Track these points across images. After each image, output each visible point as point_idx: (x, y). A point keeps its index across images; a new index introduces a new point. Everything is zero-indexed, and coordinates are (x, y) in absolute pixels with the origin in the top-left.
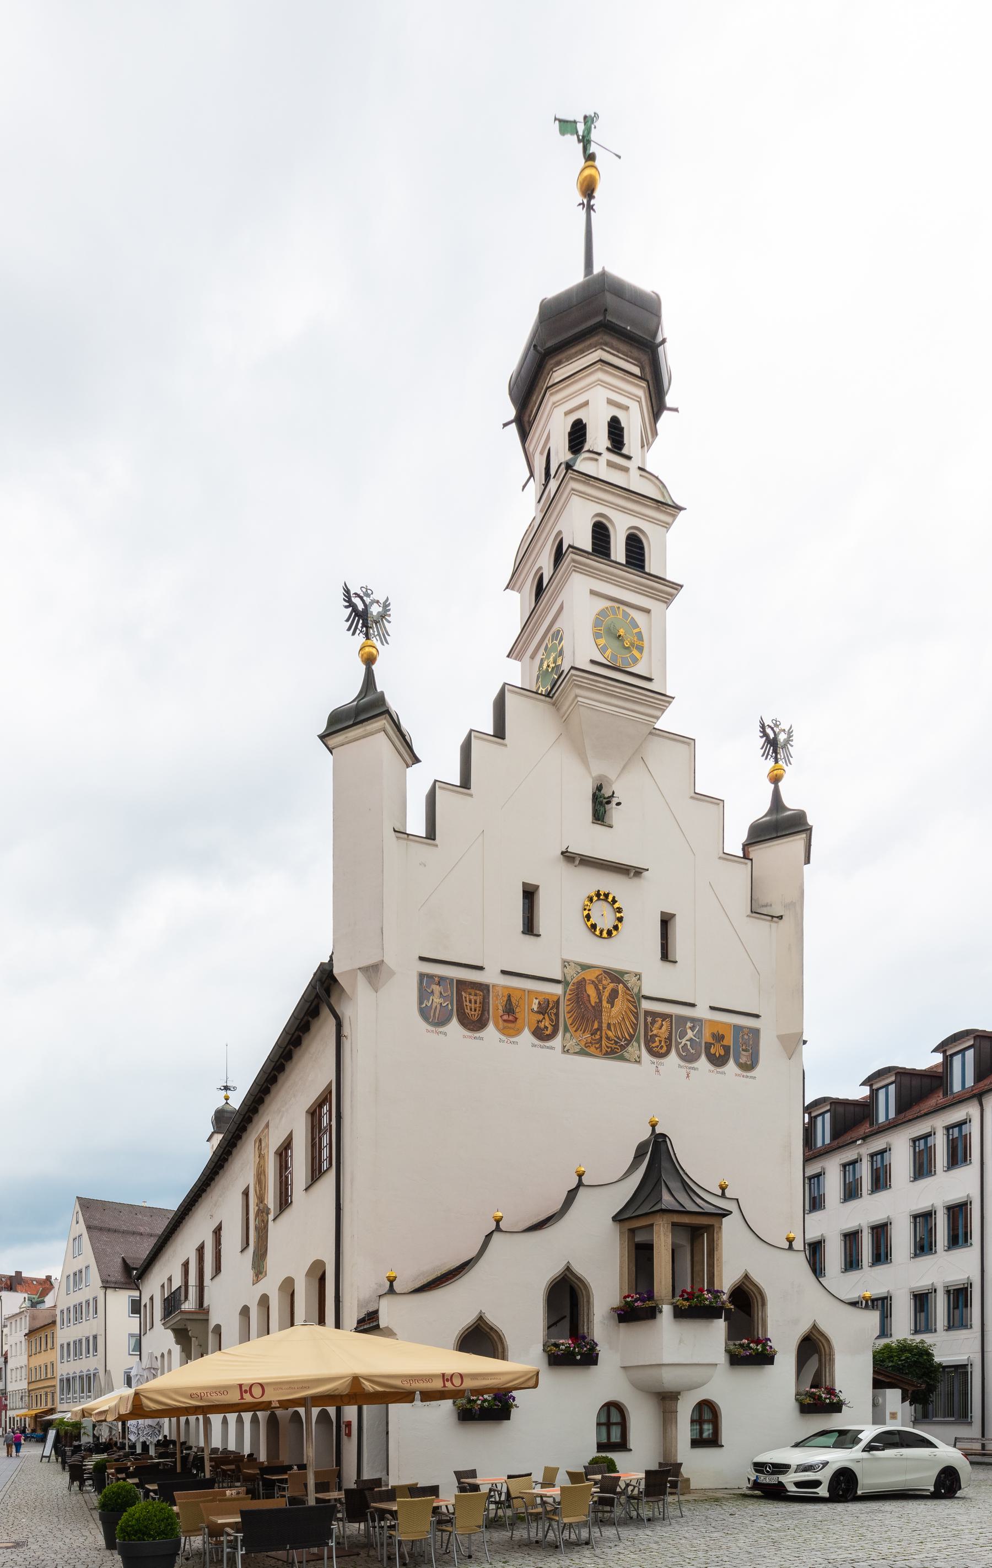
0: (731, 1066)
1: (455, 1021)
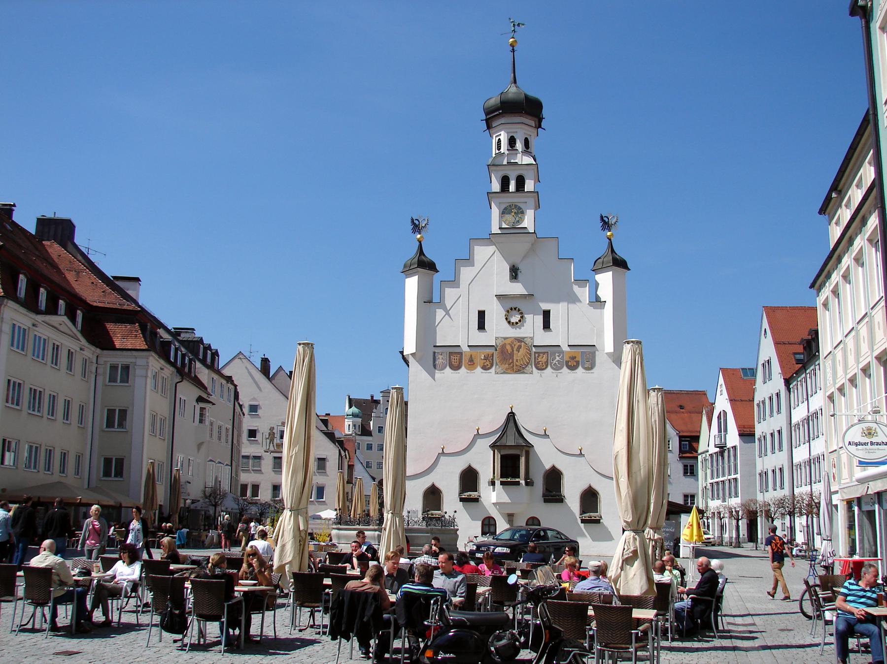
0: (580, 369)
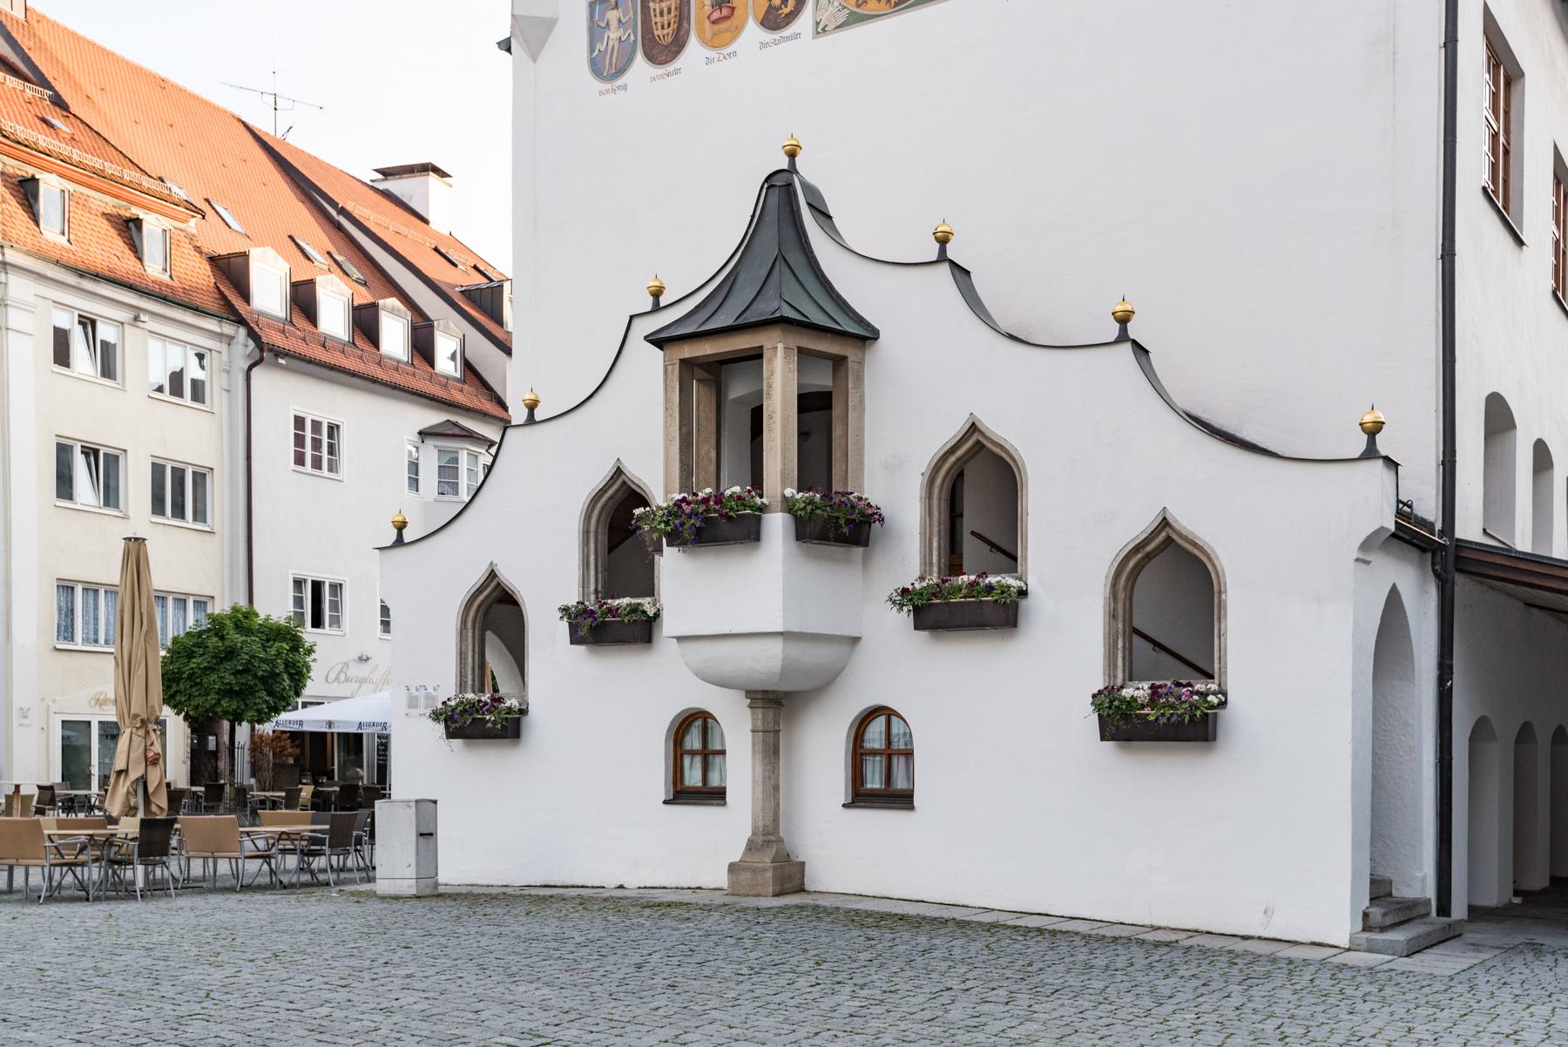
1: (640, 58)
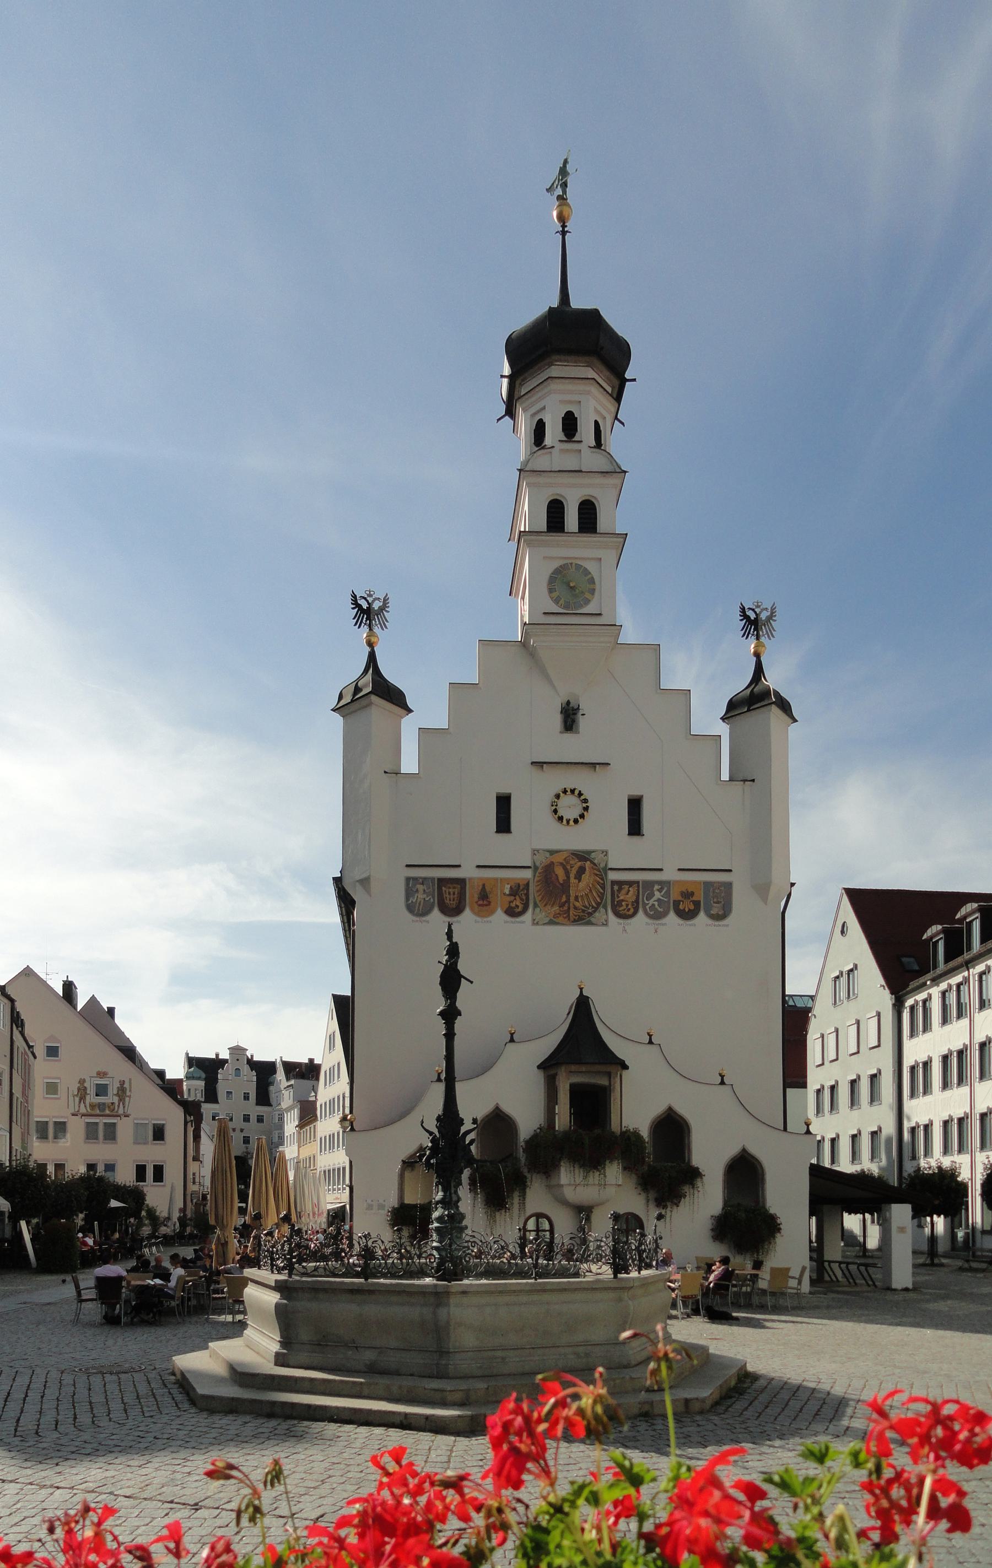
1: (436, 912)
